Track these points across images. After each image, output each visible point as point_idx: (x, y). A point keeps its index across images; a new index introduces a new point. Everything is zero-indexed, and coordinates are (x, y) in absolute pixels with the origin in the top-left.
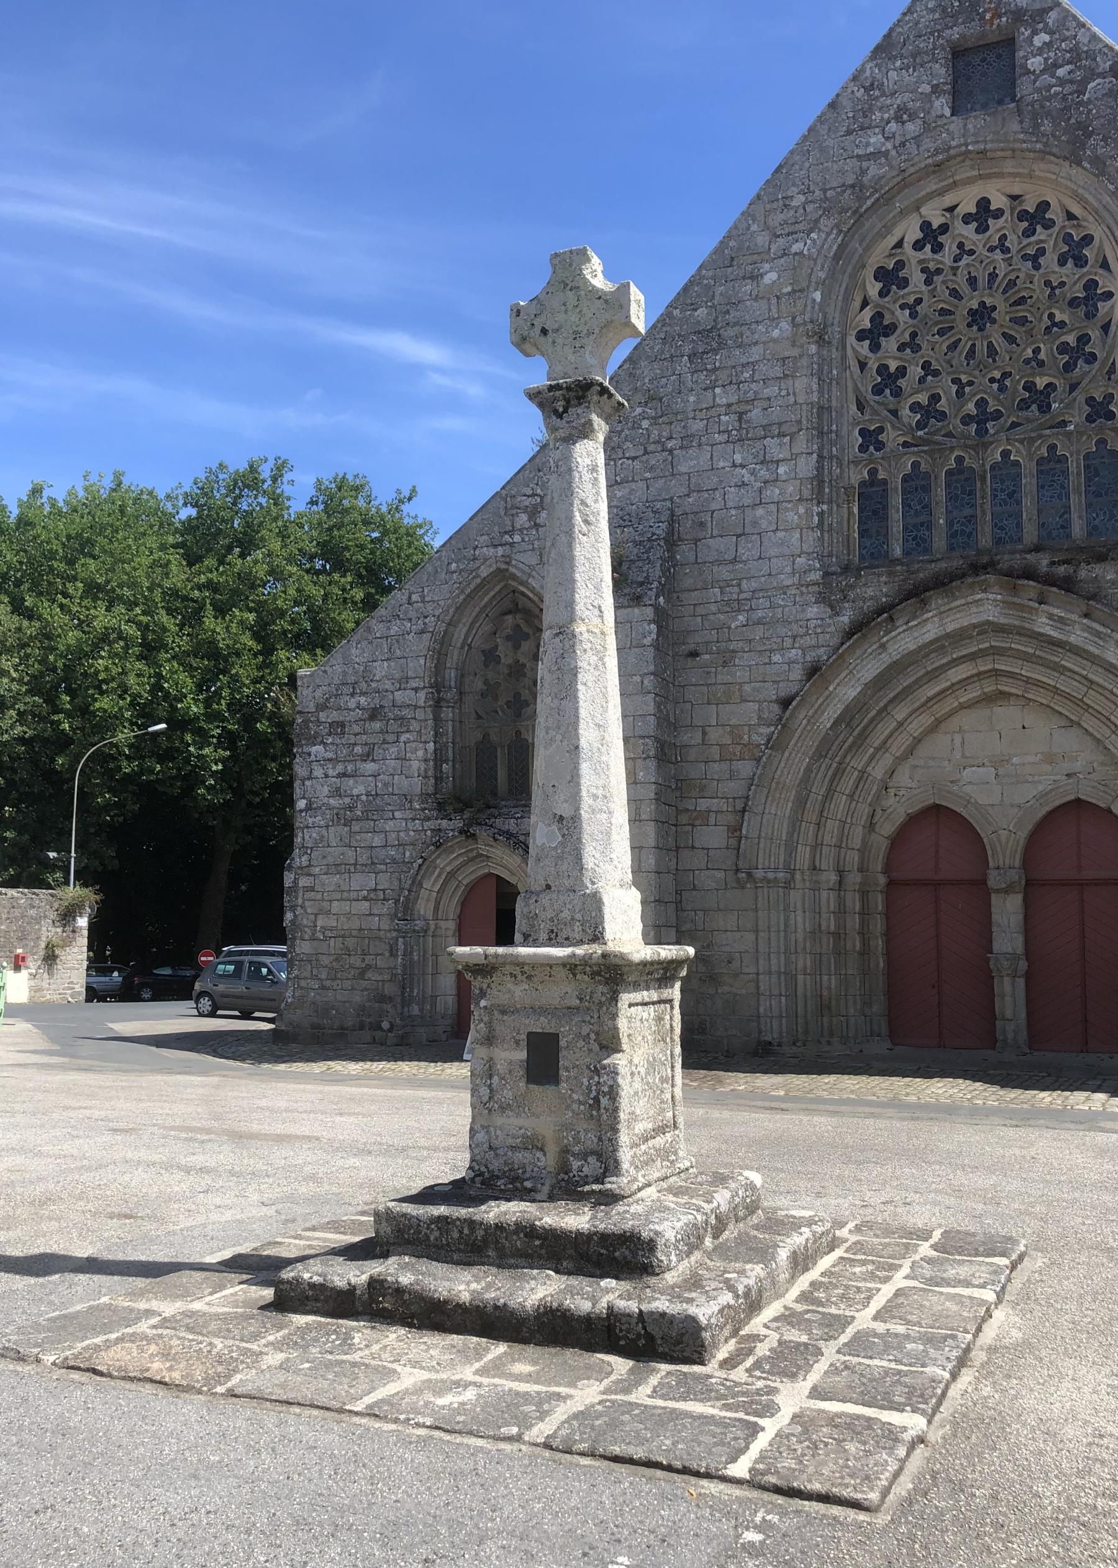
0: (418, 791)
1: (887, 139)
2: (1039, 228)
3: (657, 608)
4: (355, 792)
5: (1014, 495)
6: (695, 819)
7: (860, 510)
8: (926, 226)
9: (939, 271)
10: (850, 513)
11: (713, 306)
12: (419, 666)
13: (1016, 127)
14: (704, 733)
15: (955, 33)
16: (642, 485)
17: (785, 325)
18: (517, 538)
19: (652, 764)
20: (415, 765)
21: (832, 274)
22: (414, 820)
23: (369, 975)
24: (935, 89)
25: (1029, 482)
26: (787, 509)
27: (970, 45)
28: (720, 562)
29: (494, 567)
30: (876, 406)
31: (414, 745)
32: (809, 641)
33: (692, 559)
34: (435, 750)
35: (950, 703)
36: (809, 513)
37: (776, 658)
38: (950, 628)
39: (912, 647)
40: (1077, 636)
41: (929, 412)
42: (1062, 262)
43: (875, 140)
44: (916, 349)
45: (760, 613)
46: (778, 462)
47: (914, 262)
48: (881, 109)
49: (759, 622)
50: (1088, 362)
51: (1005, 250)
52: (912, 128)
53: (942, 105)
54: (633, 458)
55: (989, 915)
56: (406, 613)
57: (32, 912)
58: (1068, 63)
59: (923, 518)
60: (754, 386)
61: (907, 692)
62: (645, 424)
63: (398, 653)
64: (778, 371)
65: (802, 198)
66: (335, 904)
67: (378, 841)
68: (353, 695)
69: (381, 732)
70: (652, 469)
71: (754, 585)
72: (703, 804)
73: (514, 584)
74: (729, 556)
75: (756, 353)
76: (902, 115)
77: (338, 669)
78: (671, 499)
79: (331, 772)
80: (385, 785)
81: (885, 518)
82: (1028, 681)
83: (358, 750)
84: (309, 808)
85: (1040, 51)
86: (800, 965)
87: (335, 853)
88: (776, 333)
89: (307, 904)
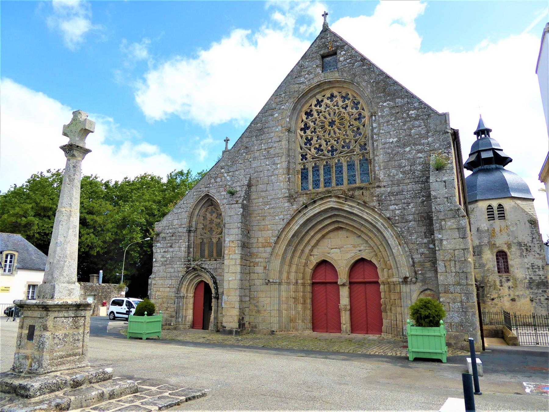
0: (183, 256)
1: (305, 79)
2: (346, 100)
3: (243, 205)
4: (167, 257)
5: (341, 172)
7: (301, 177)
8: (318, 100)
9: (321, 112)
10: (298, 177)
11: (262, 123)
12: (185, 221)
13: (337, 75)
14: (258, 240)
15: (322, 52)
16: (243, 171)
17: (280, 128)
18: (211, 186)
19: (240, 248)
20: (183, 249)
21: (292, 113)
22: (182, 264)
23: (169, 309)
24: (317, 66)
25: (345, 168)
27: (325, 55)
28: (262, 191)
31: (183, 243)
32: (285, 213)
33: (255, 190)
34: (188, 245)
35: (326, 230)
36: (285, 178)
37: (277, 218)
38: (322, 209)
39: (312, 214)
40: (355, 211)
41: (319, 149)
42: (352, 109)
43: (302, 79)
44: (315, 132)
45: (273, 205)
46: (277, 164)
47: (314, 110)
48: (304, 72)
50: (360, 135)
51: (338, 106)
52: (311, 76)
53: (319, 70)
54: (241, 164)
55: (339, 292)
56: (183, 206)
57: (109, 290)
58: (350, 58)
59: (317, 179)
60: (271, 144)
61: (313, 227)
62: (244, 154)
63: (180, 217)
64: (278, 140)
65: (284, 94)
66: (161, 289)
67: (172, 270)
68: (168, 229)
70: (245, 166)
71: (271, 197)
72: (257, 260)
74: (265, 190)
75: (272, 135)
76: (309, 73)
77: (165, 222)
78: (250, 174)
79: (162, 251)
81: (307, 179)
82: (347, 224)
83: (169, 245)
84: (156, 261)
86: (284, 308)
87: (162, 274)
88: (277, 130)
89: (154, 288)
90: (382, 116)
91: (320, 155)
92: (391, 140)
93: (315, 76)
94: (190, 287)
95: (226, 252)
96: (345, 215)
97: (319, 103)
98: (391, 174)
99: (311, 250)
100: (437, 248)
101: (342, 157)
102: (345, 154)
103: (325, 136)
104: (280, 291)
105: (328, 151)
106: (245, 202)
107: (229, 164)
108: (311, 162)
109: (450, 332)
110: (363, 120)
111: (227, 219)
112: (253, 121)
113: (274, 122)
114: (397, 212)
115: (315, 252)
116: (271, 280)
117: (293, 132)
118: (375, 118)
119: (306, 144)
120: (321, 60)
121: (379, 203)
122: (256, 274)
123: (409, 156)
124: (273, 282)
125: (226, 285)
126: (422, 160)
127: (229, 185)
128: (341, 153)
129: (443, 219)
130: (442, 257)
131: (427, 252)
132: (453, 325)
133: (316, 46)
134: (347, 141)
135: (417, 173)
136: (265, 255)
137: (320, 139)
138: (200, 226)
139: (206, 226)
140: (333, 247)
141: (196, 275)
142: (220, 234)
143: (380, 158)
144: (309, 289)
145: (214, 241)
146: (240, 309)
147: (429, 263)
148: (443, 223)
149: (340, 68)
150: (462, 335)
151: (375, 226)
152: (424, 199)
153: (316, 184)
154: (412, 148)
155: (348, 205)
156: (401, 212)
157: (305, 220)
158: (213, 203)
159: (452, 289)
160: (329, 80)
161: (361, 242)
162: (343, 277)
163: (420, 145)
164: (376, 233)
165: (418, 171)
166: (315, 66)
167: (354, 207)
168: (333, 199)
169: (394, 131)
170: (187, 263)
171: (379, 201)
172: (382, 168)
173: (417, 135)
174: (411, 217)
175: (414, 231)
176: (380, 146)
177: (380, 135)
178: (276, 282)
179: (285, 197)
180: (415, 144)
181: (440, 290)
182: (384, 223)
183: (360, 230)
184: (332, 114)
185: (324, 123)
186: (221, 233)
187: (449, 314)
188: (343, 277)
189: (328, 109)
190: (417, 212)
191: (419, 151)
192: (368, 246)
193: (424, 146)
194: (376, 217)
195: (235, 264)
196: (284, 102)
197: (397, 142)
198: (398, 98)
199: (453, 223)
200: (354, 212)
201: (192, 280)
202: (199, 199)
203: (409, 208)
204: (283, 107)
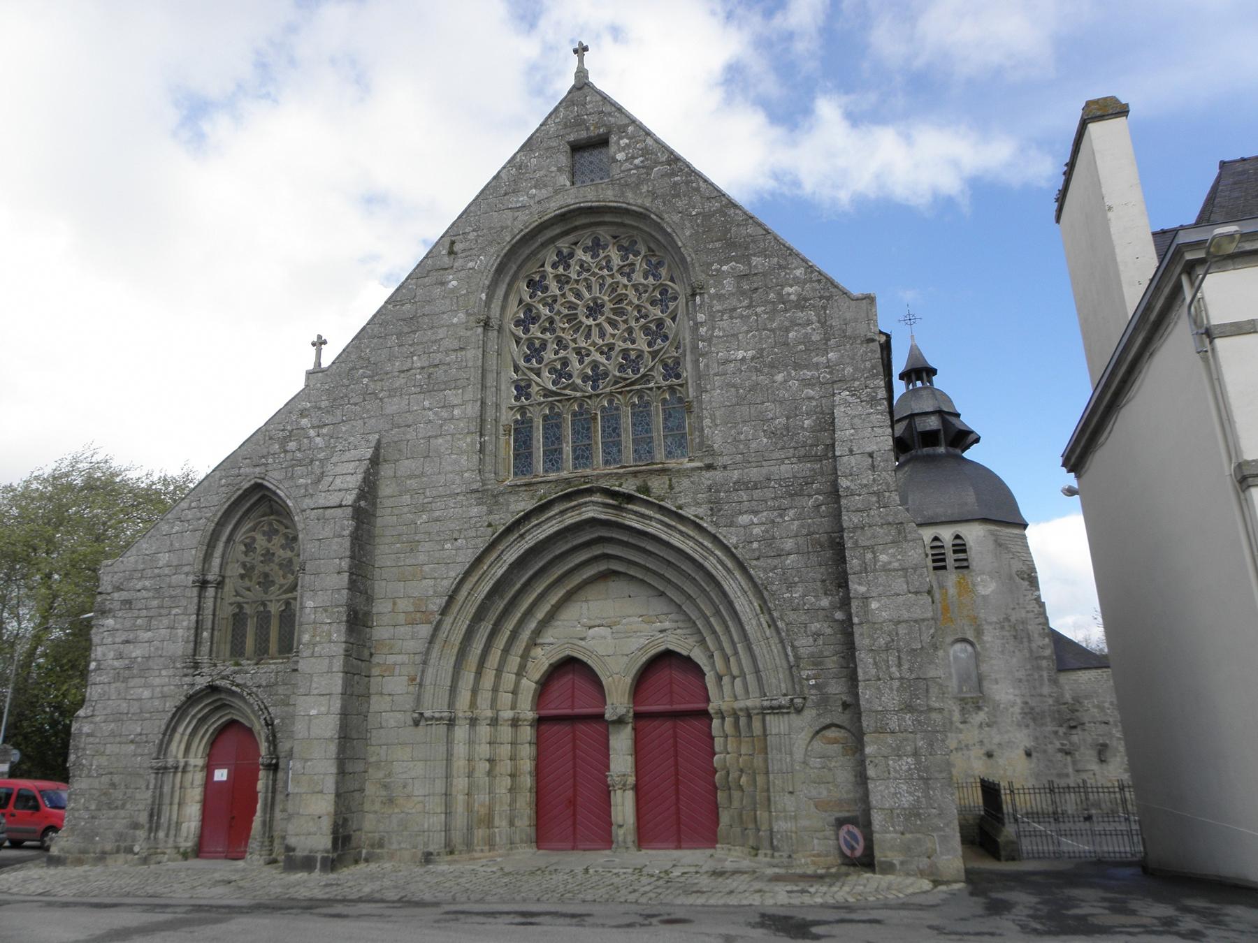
0: (180, 653)
4: (134, 655)
6: (385, 671)
9: (567, 282)
12: (193, 555)
14: (394, 604)
15: (572, 138)
16: (361, 422)
17: (462, 315)
18: (270, 461)
19: (343, 628)
20: (180, 632)
24: (560, 170)
26: (459, 439)
28: (410, 477)
29: (252, 482)
30: (526, 371)
31: (181, 617)
33: (392, 474)
36: (473, 443)
37: (448, 546)
38: (568, 522)
41: (561, 372)
44: (553, 331)
45: (437, 513)
46: (453, 406)
47: (551, 276)
49: (437, 520)
53: (564, 180)
54: (356, 404)
62: (365, 381)
63: (177, 545)
64: (456, 345)
65: (475, 234)
67: (146, 694)
69: (159, 607)
72: (391, 659)
73: (269, 494)
75: (441, 333)
80: (157, 649)
84: (98, 669)
85: (623, 149)
88: (455, 320)
90: (720, 297)
91: (564, 388)
92: (740, 354)
93: (556, 192)
94: (197, 740)
95: (306, 638)
96: (625, 539)
97: (564, 259)
98: (742, 437)
99: (538, 632)
100: (856, 620)
101: (620, 393)
102: (623, 387)
103: (578, 341)
104: (449, 742)
105: (585, 378)
106: (363, 503)
107: (324, 404)
108: (540, 404)
109: (890, 832)
110: (672, 306)
111: (308, 547)
112: (389, 299)
113: (448, 302)
114: (757, 531)
115: (548, 637)
116: (428, 714)
117: (496, 327)
118: (702, 301)
119: (528, 359)
120: (569, 155)
121: (712, 509)
122: (388, 699)
123: (782, 393)
124: (433, 718)
125: (300, 728)
126: (814, 403)
127: (320, 460)
128: (616, 383)
129: (868, 547)
130: (867, 642)
131: (829, 631)
132: (898, 815)
133: (557, 120)
134: (633, 355)
135: (803, 436)
136: (411, 645)
137: (565, 348)
138: (234, 570)
139: (253, 568)
140: (593, 623)
141: (218, 704)
142: (291, 592)
143: (715, 398)
144: (527, 733)
145: (274, 608)
146: (338, 795)
147: (835, 658)
148: (869, 556)
149: (617, 177)
150: (918, 840)
151: (701, 567)
152: (821, 498)
153: (553, 456)
154: (789, 374)
155: (635, 513)
156: (767, 531)
157: (522, 551)
158: (275, 506)
159: (893, 724)
160: (590, 204)
161: (666, 610)
162: (618, 702)
163: (807, 367)
164: (703, 584)
165: (806, 430)
166: (554, 169)
167: (650, 518)
168: (597, 498)
169: (747, 332)
170: (190, 671)
171: (710, 502)
172: (718, 422)
173: (801, 343)
174: (789, 544)
175: (796, 579)
176: (715, 368)
177: (715, 341)
178: (441, 718)
179: (473, 491)
180: (797, 366)
181: (865, 724)
182: (724, 558)
183: (662, 577)
184: (596, 288)
185: (576, 309)
186: (293, 588)
187: (887, 787)
188: (618, 702)
189: (585, 275)
190: (804, 531)
191: (808, 383)
192: (682, 618)
193: (818, 370)
194: (706, 543)
195: (330, 672)
196: (474, 252)
197: (753, 358)
198: (754, 255)
199: (894, 556)
200: (650, 530)
201: (203, 720)
202: (236, 496)
203: (785, 521)
204: (471, 264)
